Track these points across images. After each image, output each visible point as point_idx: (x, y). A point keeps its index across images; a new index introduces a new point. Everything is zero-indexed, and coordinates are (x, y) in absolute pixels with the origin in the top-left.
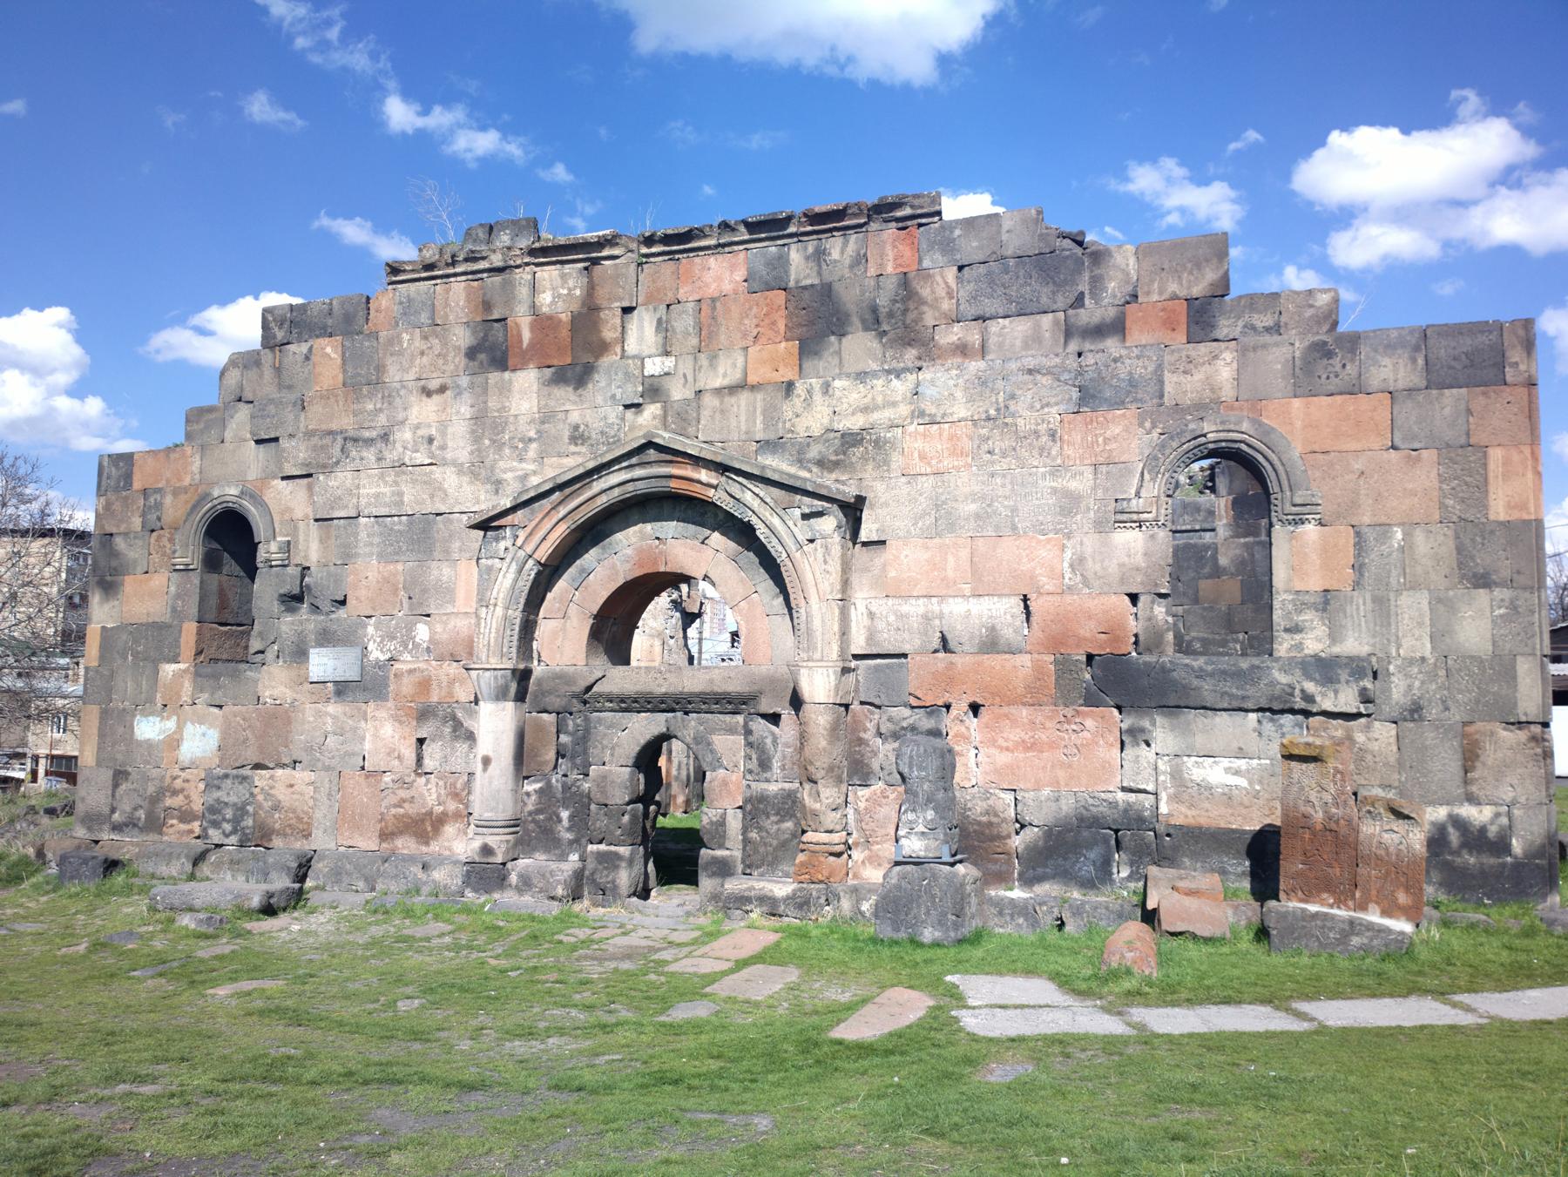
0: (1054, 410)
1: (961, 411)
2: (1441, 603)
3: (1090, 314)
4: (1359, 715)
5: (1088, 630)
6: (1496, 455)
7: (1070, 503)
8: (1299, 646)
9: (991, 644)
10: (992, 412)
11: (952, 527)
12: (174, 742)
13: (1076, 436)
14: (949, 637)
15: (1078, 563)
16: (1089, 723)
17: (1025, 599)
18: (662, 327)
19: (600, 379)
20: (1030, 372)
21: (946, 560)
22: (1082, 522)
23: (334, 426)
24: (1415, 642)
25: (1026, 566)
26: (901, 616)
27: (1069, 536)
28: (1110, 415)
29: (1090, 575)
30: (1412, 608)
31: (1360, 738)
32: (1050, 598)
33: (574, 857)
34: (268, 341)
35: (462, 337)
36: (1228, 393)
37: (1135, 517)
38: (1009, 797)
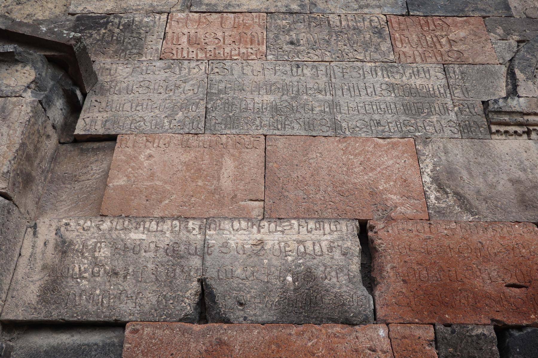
0: (377, 11)
5: (489, 279)
7: (417, 104)
10: (295, 7)
11: (232, 122)
13: (409, 41)
14: (218, 289)
17: (364, 230)
21: (219, 165)
22: (442, 123)
25: (361, 178)
26: (122, 249)
27: (426, 140)
28: (449, 20)
29: (469, 193)
32: (410, 225)
37: (520, 119)
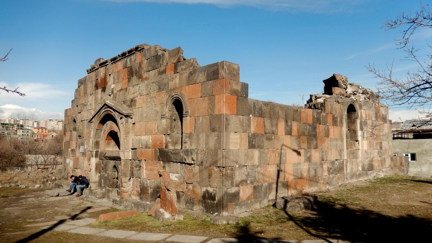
1: (145, 93)
2: (207, 136)
3: (162, 69)
4: (192, 164)
5: (158, 143)
6: (217, 97)
8: (186, 147)
9: (147, 147)
12: (69, 163)
15: (158, 127)
16: (158, 165)
18: (114, 78)
19: (106, 90)
20: (153, 83)
23: (83, 103)
24: (203, 146)
26: (136, 140)
30: (203, 136)
31: (193, 170)
33: (104, 190)
34: (79, 87)
35: (94, 83)
36: (178, 86)
38: (149, 181)
